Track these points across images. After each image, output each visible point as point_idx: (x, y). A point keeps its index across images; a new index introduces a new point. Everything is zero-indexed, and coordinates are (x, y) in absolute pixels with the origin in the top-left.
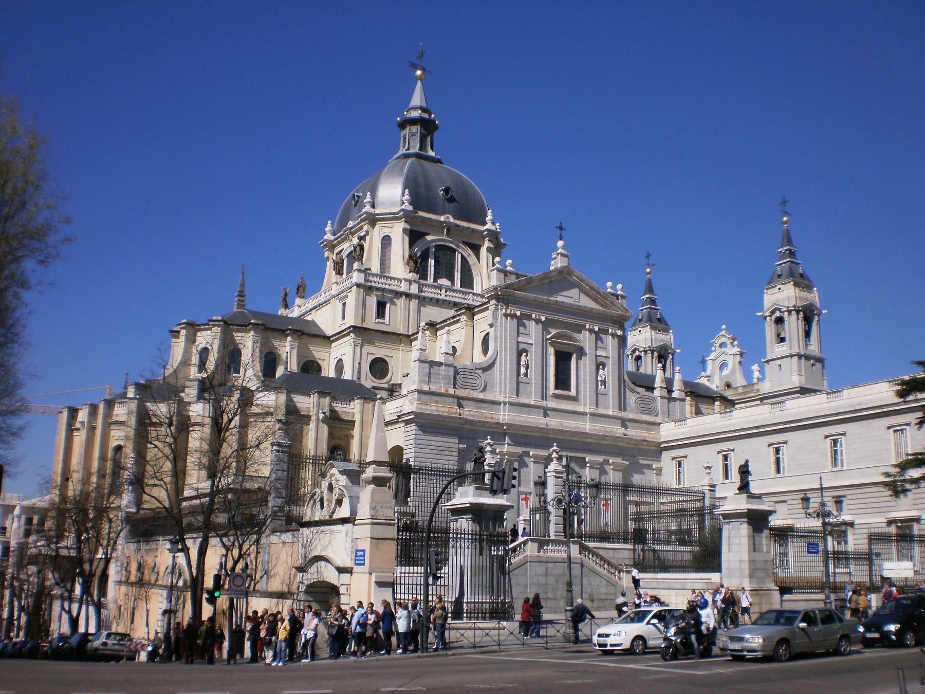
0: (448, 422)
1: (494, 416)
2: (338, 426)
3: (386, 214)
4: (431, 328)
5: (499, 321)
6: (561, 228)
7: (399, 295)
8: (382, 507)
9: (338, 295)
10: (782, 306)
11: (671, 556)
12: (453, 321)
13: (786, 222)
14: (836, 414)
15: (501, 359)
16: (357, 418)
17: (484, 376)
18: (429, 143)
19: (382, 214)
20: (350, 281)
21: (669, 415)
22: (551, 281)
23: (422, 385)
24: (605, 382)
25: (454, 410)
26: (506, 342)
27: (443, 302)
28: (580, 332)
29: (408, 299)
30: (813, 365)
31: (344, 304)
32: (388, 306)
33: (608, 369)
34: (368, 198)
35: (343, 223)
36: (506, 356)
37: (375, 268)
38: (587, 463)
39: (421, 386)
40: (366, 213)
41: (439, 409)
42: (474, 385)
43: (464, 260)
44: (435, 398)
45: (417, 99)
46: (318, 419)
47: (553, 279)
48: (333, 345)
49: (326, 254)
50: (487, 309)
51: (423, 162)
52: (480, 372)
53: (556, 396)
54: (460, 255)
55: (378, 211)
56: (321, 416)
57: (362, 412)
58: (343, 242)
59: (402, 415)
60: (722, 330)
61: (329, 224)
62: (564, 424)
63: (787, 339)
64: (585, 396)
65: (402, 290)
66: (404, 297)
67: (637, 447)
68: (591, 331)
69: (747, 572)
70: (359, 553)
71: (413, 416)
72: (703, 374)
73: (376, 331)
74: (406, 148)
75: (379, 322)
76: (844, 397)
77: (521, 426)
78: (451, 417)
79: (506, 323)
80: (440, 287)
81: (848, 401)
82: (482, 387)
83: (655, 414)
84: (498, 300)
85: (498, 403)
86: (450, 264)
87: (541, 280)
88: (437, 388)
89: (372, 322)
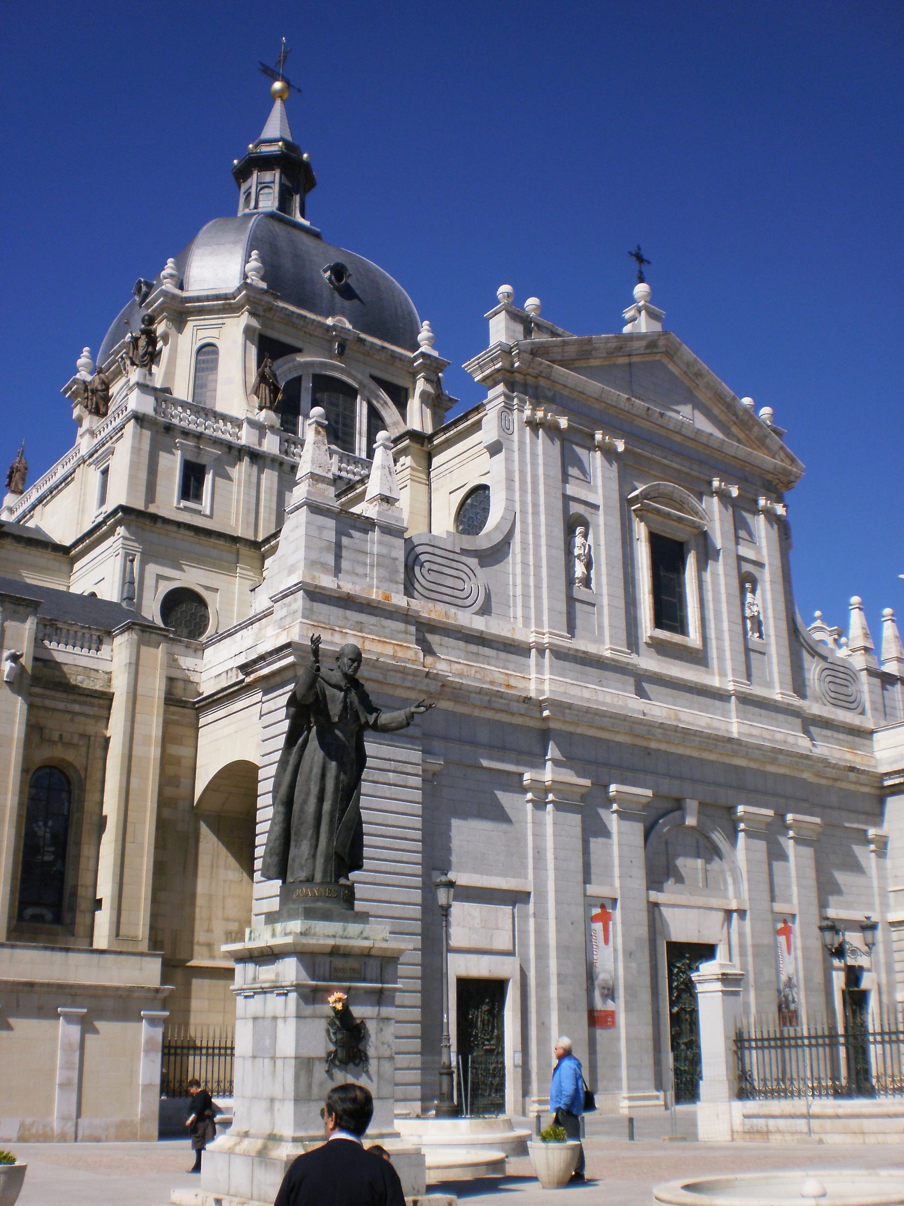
0: (395, 686)
1: (513, 682)
2: (61, 706)
5: (516, 436)
6: (640, 259)
9: (91, 456)
15: (524, 532)
16: (120, 687)
18: (298, 205)
21: (885, 715)
22: (630, 364)
23: (316, 574)
24: (760, 624)
25: (410, 654)
26: (535, 492)
28: (700, 496)
33: (763, 592)
36: (536, 526)
37: (182, 390)
38: (741, 820)
39: (313, 578)
42: (457, 593)
47: (635, 359)
48: (77, 566)
52: (473, 562)
57: (135, 667)
59: (255, 662)
62: (683, 717)
64: (720, 650)
65: (243, 442)
67: (839, 785)
68: (724, 496)
71: (291, 659)
73: (180, 525)
75: (186, 509)
77: (588, 710)
78: (403, 671)
83: (859, 710)
84: (511, 386)
86: (344, 418)
87: (610, 354)
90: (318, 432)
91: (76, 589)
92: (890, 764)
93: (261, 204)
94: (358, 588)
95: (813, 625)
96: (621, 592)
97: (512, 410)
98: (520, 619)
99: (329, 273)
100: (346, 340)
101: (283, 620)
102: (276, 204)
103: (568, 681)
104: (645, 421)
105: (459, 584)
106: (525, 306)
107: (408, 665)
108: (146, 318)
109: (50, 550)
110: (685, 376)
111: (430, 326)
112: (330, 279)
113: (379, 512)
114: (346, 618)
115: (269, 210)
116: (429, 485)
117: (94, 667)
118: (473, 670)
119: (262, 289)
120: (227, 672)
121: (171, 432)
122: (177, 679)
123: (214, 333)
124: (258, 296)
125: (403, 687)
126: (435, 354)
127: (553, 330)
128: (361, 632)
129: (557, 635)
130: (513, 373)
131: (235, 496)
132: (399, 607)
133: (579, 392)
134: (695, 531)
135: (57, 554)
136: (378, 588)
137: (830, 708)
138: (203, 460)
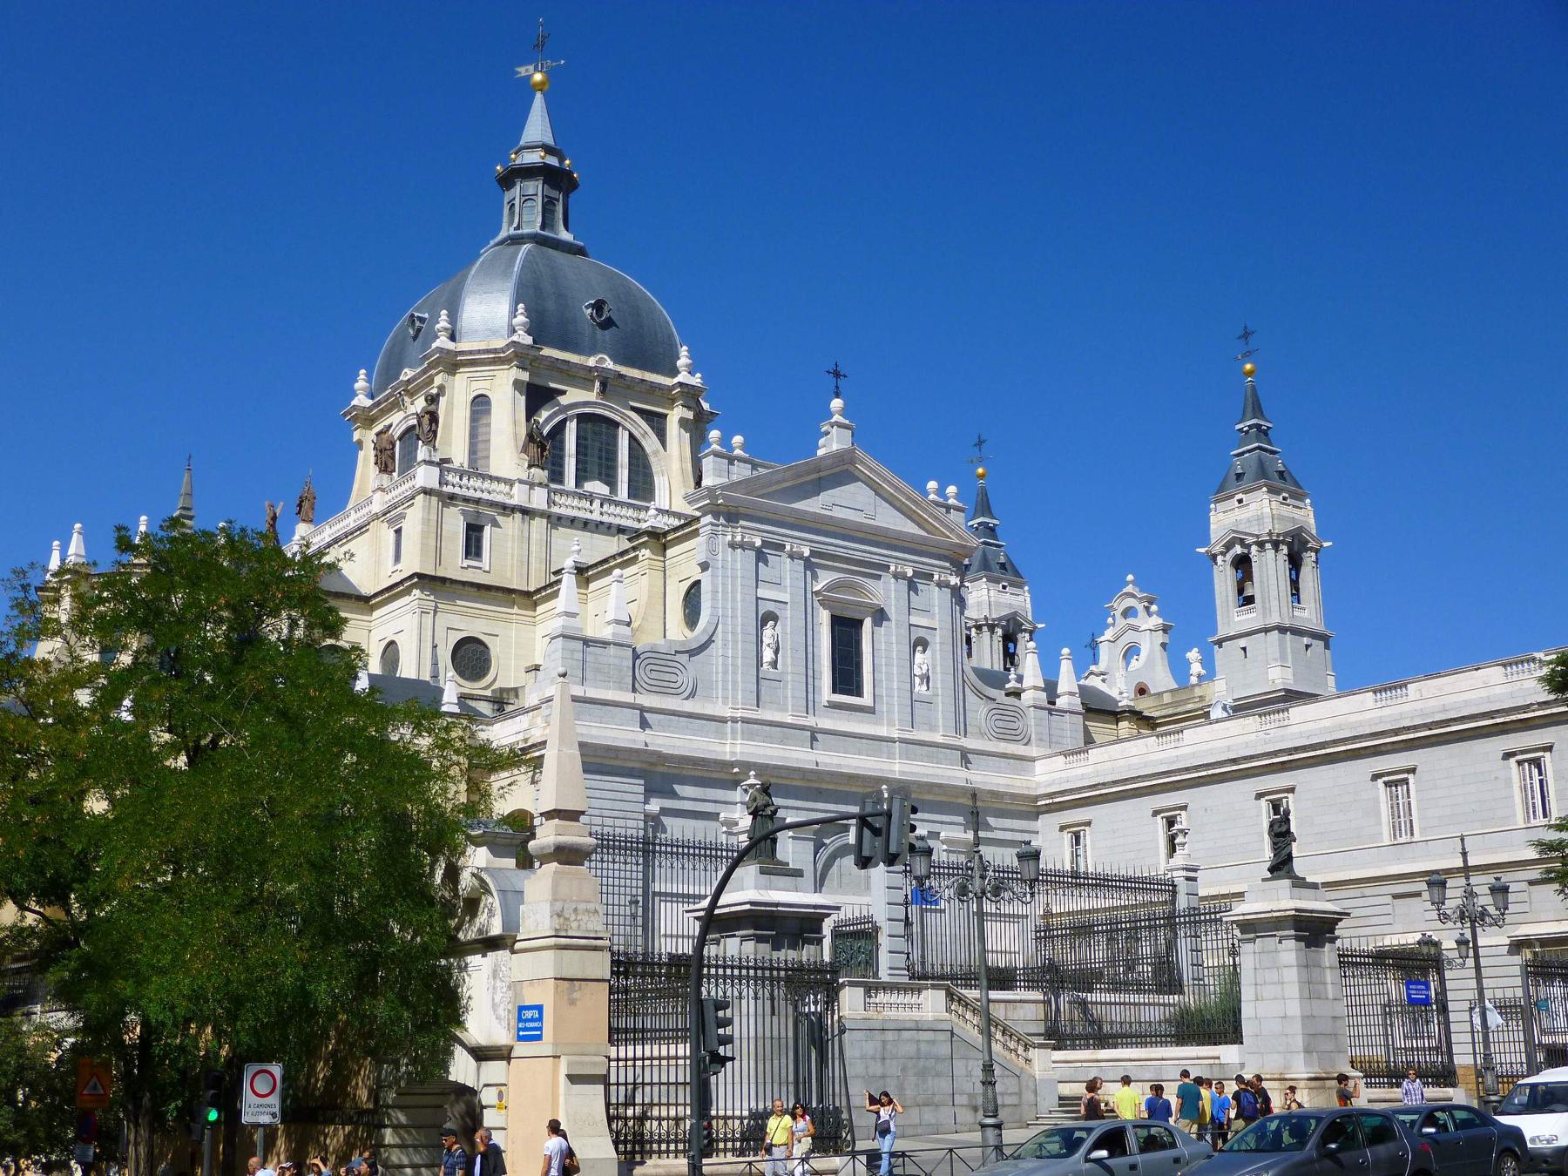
3: (479, 352)
5: (720, 557)
6: (837, 374)
8: (575, 910)
10: (1246, 534)
11: (1116, 1014)
12: (625, 559)
13: (1250, 373)
14: (1396, 732)
17: (694, 665)
18: (561, 216)
19: (471, 352)
20: (410, 484)
26: (734, 600)
29: (527, 518)
30: (1307, 647)
31: (398, 532)
34: (443, 322)
35: (390, 372)
40: (440, 350)
42: (672, 685)
43: (635, 444)
45: (537, 127)
48: (377, 614)
49: (356, 436)
50: (695, 533)
51: (550, 250)
52: (684, 658)
53: (834, 706)
55: (463, 346)
58: (390, 410)
59: (531, 747)
60: (1127, 583)
61: (362, 377)
63: (1257, 599)
65: (514, 501)
69: (1299, 1042)
70: (528, 1014)
72: (1093, 668)
73: (464, 583)
74: (515, 225)
75: (469, 566)
76: (1411, 698)
79: (734, 561)
80: (590, 497)
81: (1419, 705)
82: (689, 690)
83: (1025, 741)
84: (716, 515)
85: (723, 720)
89: (455, 565)
92: (1046, 786)
95: (1125, 590)
99: (590, 311)
105: (673, 677)
116: (665, 571)
123: (486, 384)
124: (525, 351)
137: (995, 742)
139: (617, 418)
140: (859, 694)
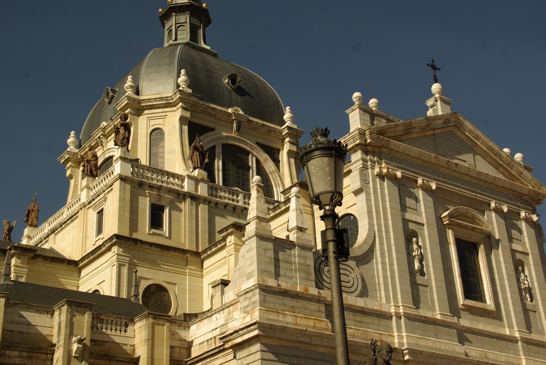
0: (317, 345)
4: (237, 233)
6: (434, 67)
7: (181, 197)
18: (202, 36)
22: (434, 134)
23: (265, 278)
25: (323, 325)
27: (242, 210)
32: (167, 211)
36: (388, 239)
39: (264, 281)
41: (299, 321)
44: (289, 302)
46: (68, 351)
47: (437, 131)
48: (84, 272)
49: (68, 173)
53: (469, 309)
54: (254, 159)
56: (75, 347)
57: (152, 341)
61: (72, 135)
62: (490, 356)
65: (186, 189)
66: (188, 201)
68: (498, 211)
73: (151, 244)
75: (154, 234)
77: (432, 355)
84: (366, 152)
87: (423, 129)
88: (289, 285)
90: (258, 191)
91: (83, 288)
93: (179, 37)
94: (289, 285)
96: (442, 277)
97: (367, 169)
98: (384, 299)
100: (241, 121)
101: (247, 308)
102: (188, 36)
103: (416, 336)
104: (446, 169)
106: (369, 104)
107: (324, 332)
108: (123, 116)
109: (66, 264)
110: (468, 139)
111: (290, 109)
112: (228, 83)
113: (297, 237)
114: (284, 304)
115: (185, 41)
117: (124, 343)
118: (360, 332)
119: (190, 93)
120: (208, 341)
121: (142, 187)
122: (175, 347)
123: (161, 121)
125: (322, 346)
126: (295, 127)
127: (387, 118)
128: (294, 312)
129: (407, 307)
130: (366, 146)
131: (183, 224)
132: (314, 295)
133: (406, 155)
134: (483, 235)
135: (71, 266)
136: (300, 284)
138: (162, 204)
139: (248, 149)
140: (485, 302)
